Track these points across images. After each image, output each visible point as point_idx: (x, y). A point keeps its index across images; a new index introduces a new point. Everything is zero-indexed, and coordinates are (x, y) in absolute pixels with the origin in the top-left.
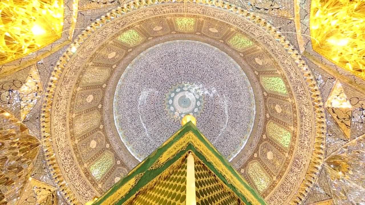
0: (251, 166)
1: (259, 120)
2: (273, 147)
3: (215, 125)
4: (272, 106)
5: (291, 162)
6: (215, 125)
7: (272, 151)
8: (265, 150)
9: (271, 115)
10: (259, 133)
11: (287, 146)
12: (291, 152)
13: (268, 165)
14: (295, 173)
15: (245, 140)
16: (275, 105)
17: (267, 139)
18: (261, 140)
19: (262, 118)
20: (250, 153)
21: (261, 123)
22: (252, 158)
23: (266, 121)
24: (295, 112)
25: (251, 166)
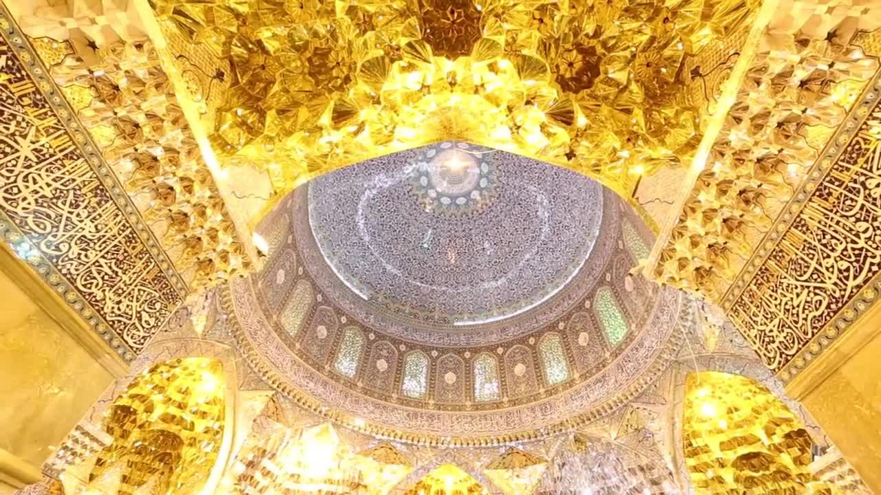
2: (533, 366)
3: (471, 250)
4: (579, 326)
6: (471, 250)
7: (527, 367)
8: (518, 357)
10: (528, 326)
11: (551, 383)
12: (548, 393)
13: (508, 380)
15: (499, 314)
17: (533, 347)
18: (523, 341)
19: (552, 316)
20: (494, 338)
21: (543, 320)
22: (491, 349)
23: (552, 327)
24: (598, 369)
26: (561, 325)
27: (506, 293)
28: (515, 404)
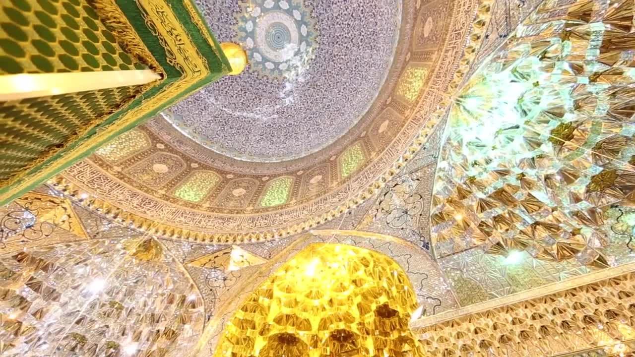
0: (140, 135)
1: (224, 163)
4: (244, 184)
5: (150, 196)
9: (231, 181)
10: (202, 157)
11: (177, 194)
12: (166, 198)
13: (142, 163)
14: (130, 199)
15: (189, 133)
16: (246, 188)
18: (188, 160)
19: (228, 168)
20: (166, 138)
21: (218, 164)
22: (155, 139)
23: (222, 172)
24: (231, 212)
25: (140, 135)
26: (229, 176)
27: (211, 132)
28: (121, 179)
